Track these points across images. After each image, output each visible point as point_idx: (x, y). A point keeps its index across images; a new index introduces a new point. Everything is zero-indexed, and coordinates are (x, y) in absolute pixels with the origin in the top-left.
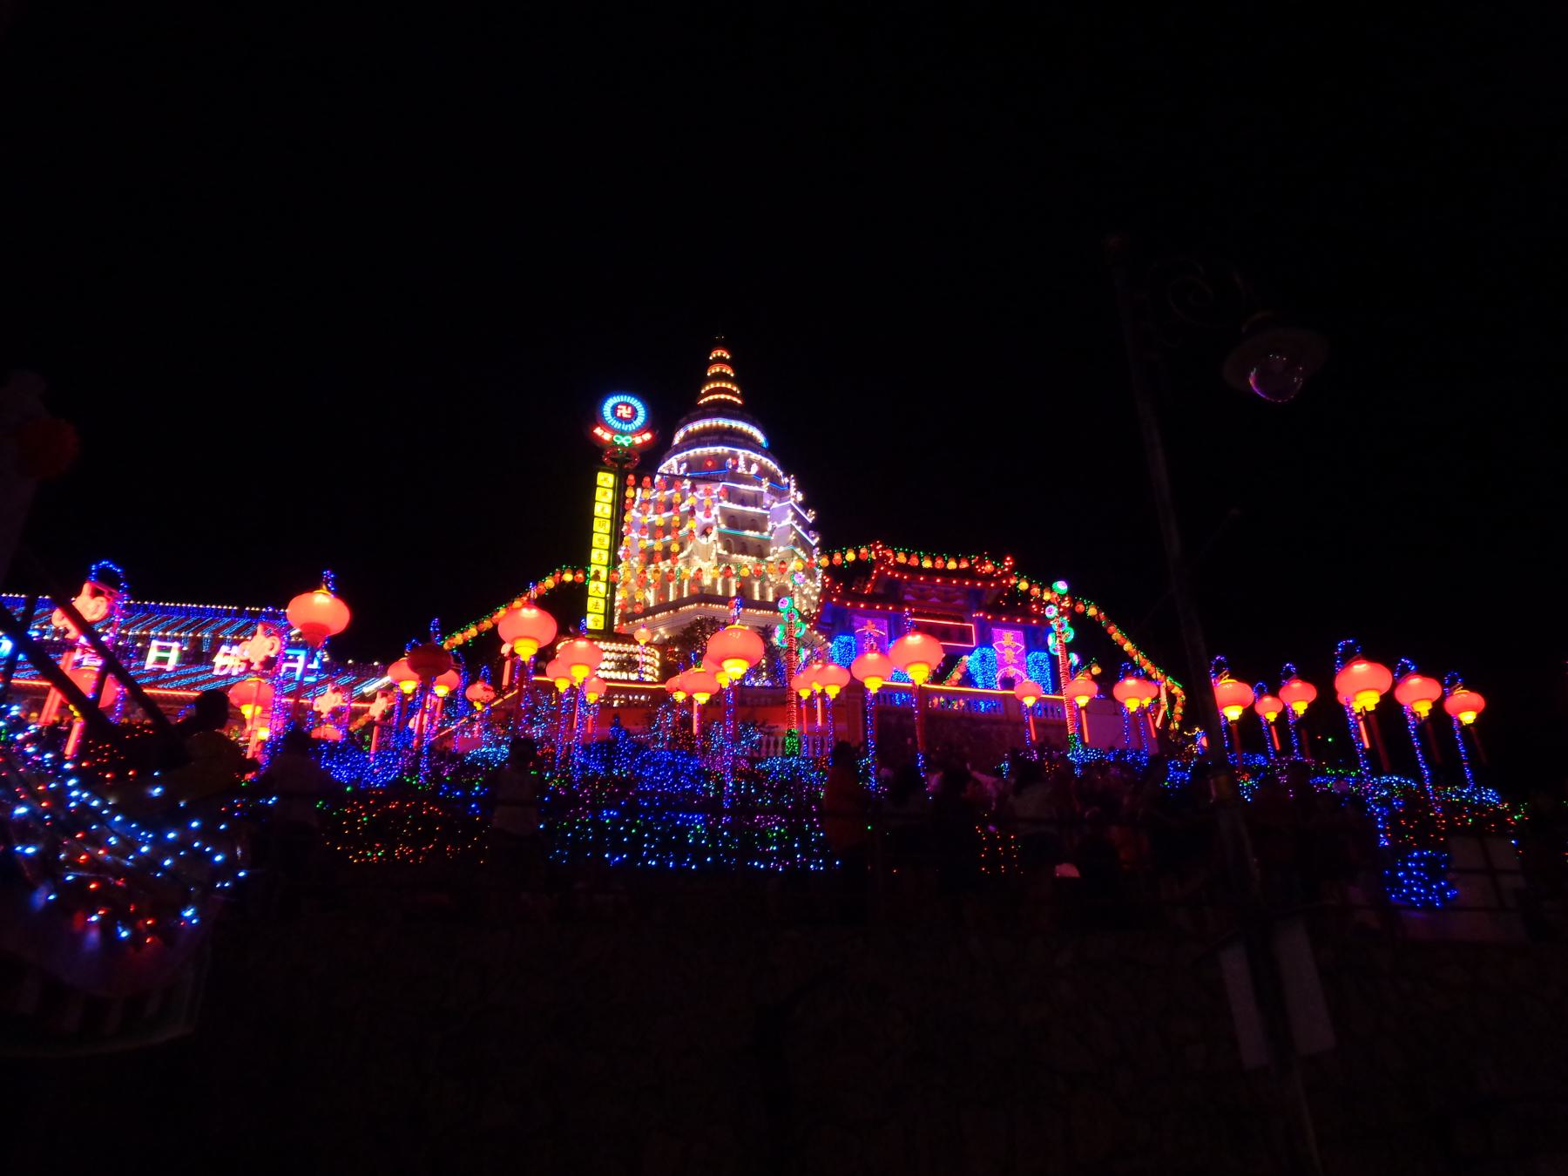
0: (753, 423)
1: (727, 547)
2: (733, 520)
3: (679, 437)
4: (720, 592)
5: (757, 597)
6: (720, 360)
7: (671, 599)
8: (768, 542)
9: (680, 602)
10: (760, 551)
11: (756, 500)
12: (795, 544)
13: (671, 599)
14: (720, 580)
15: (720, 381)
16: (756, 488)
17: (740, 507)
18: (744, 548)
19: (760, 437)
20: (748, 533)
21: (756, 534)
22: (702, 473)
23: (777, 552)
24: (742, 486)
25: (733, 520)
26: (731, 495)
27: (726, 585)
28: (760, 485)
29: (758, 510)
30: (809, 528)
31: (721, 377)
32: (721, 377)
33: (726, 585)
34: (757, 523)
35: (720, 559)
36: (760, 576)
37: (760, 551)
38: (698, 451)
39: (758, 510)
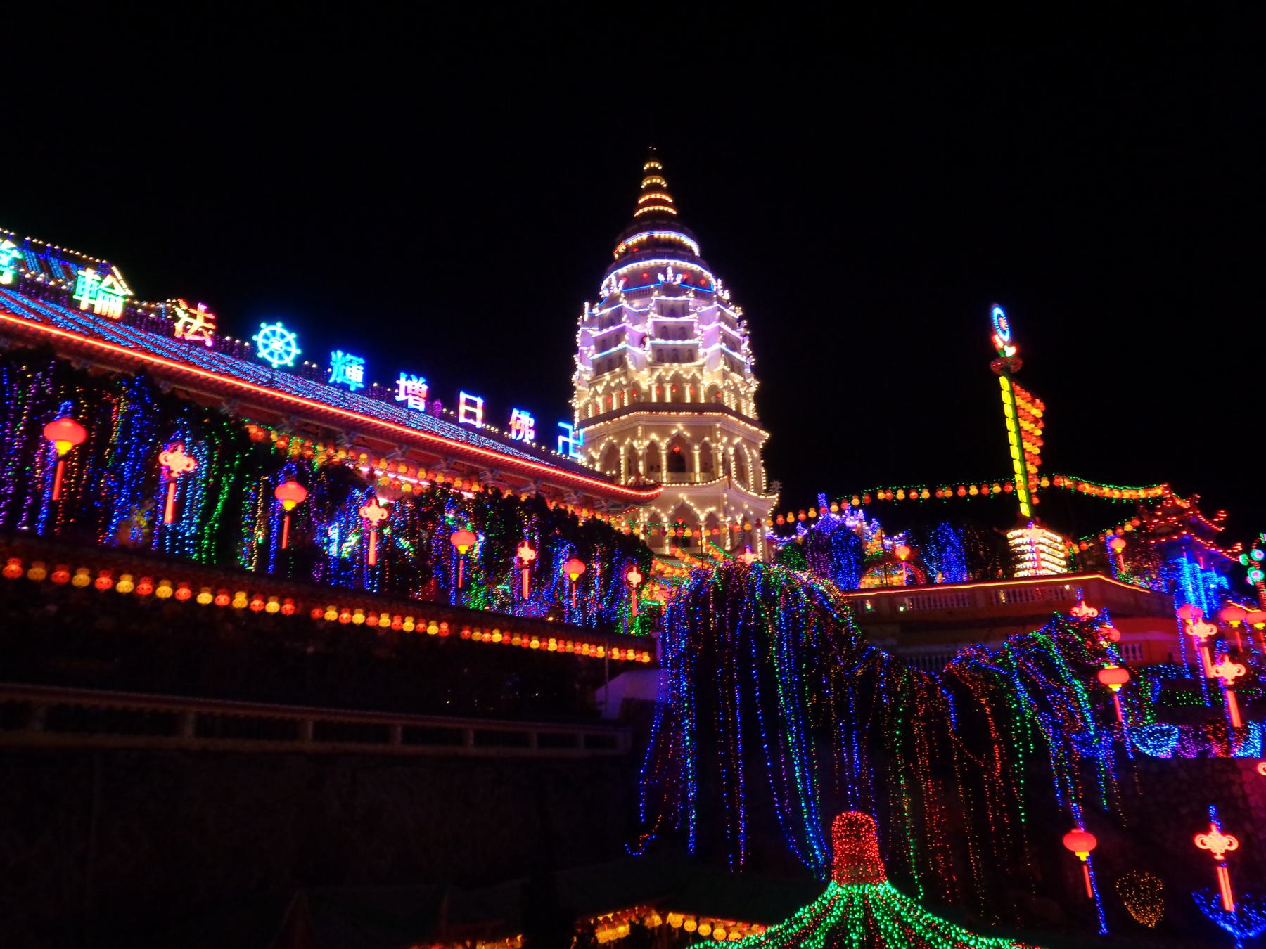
0: (681, 231)
3: (621, 248)
4: (654, 399)
5: (688, 400)
6: (653, 172)
7: (615, 408)
9: (622, 410)
10: (689, 355)
13: (615, 408)
14: (654, 387)
15: (655, 196)
18: (677, 356)
22: (638, 285)
25: (663, 331)
27: (661, 390)
30: (732, 324)
31: (655, 188)
32: (655, 188)
33: (661, 390)
34: (685, 332)
38: (635, 265)
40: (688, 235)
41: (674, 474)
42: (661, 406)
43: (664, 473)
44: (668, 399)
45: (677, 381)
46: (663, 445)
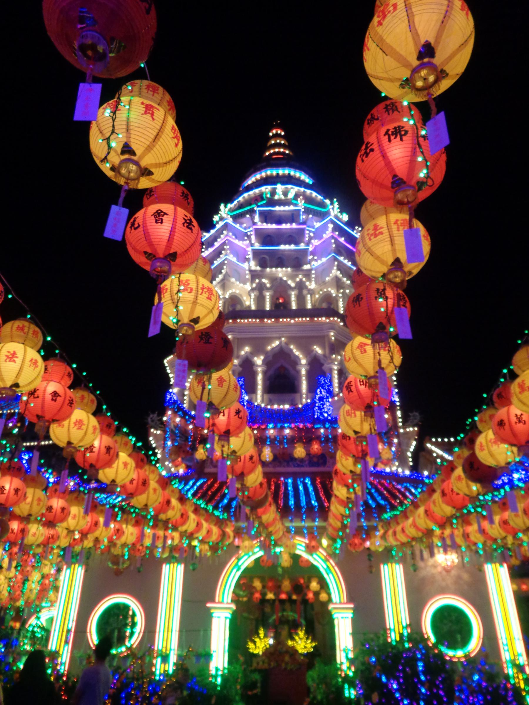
1: (263, 264)
2: (267, 238)
8: (305, 252)
10: (296, 262)
11: (293, 217)
12: (339, 253)
16: (292, 208)
17: (274, 226)
18: (280, 261)
19: (308, 180)
20: (282, 247)
21: (293, 247)
23: (316, 264)
24: (277, 208)
25: (267, 238)
26: (266, 217)
28: (296, 205)
29: (294, 226)
33: (260, 299)
35: (254, 275)
36: (301, 286)
37: (296, 262)
39: (294, 226)
40: (306, 173)
41: (271, 396)
42: (260, 314)
43: (259, 392)
44: (268, 307)
45: (280, 289)
46: (259, 361)
